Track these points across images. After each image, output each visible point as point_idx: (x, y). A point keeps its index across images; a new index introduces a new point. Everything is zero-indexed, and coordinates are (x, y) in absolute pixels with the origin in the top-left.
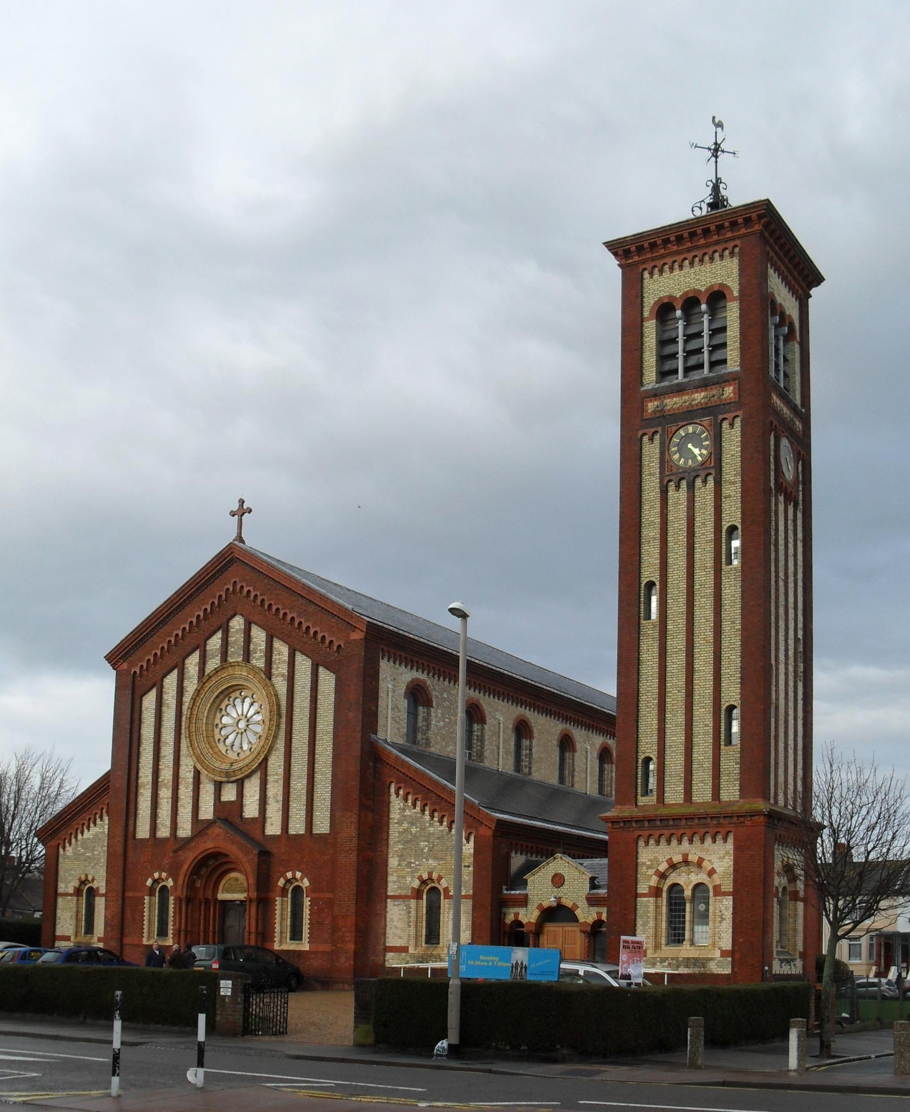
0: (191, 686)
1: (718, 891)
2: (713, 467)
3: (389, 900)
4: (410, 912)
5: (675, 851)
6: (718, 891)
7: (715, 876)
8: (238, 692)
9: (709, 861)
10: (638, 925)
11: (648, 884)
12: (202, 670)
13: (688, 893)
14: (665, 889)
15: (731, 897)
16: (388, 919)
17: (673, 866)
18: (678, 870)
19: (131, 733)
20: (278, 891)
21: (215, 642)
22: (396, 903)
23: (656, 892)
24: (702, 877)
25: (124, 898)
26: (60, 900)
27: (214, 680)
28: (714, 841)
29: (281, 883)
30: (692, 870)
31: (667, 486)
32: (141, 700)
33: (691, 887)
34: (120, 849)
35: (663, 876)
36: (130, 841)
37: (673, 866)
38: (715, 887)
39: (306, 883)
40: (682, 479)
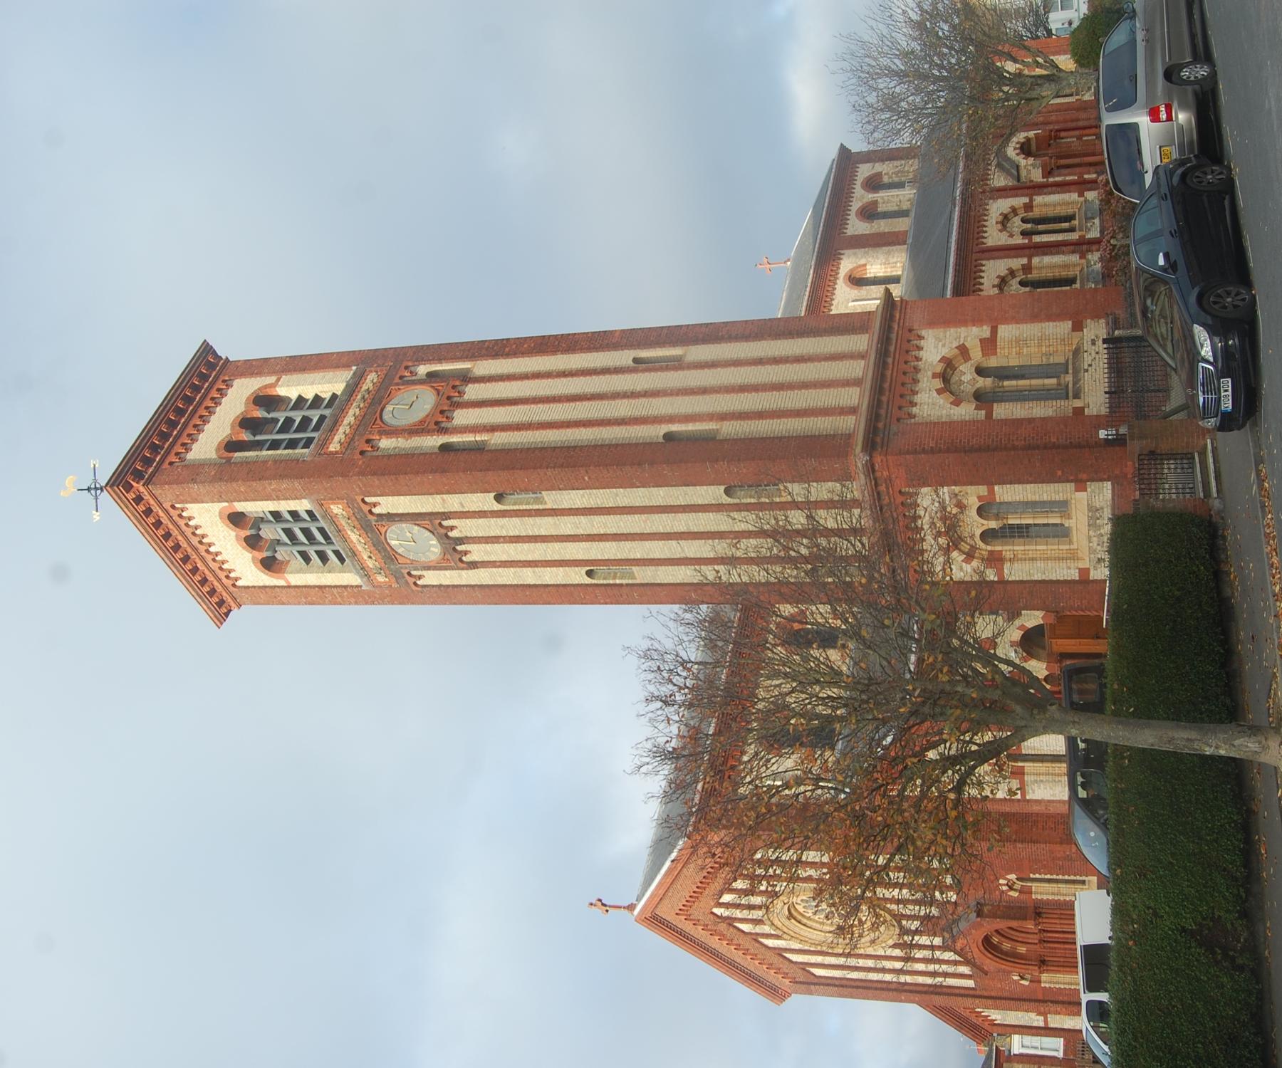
0: (796, 946)
2: (431, 521)
3: (1027, 798)
4: (1042, 781)
8: (797, 906)
10: (1044, 578)
12: (777, 937)
15: (996, 488)
16: (1052, 798)
19: (858, 987)
20: (1024, 897)
21: (746, 927)
22: (1030, 791)
25: (1046, 1002)
26: (1051, 1025)
27: (786, 930)
29: (1014, 894)
31: (467, 563)
32: (820, 977)
34: (990, 1002)
36: (978, 993)
39: (1013, 877)
40: (454, 549)
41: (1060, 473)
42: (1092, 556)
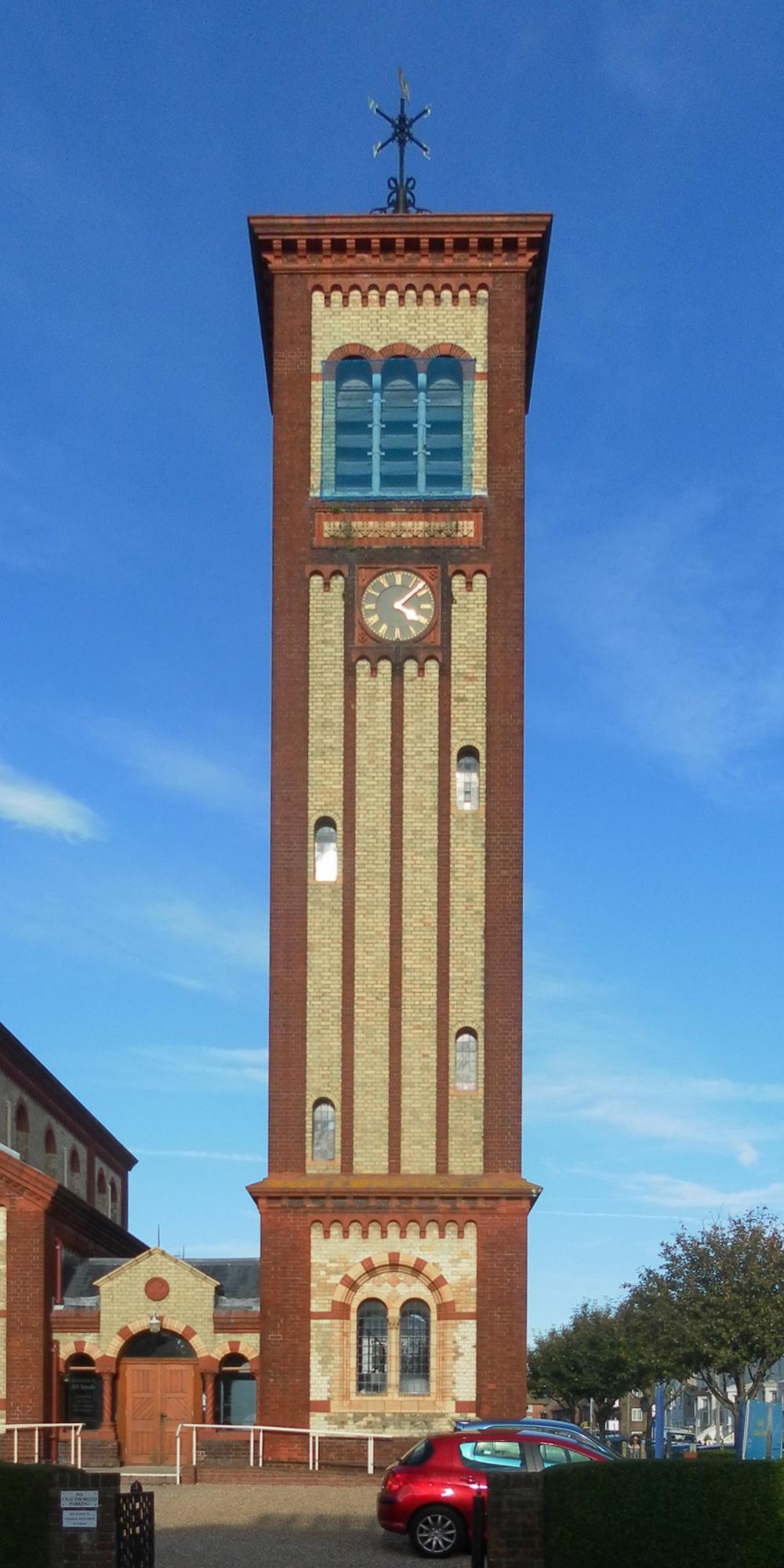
1: (447, 1312)
5: (377, 1247)
6: (447, 1312)
7: (444, 1289)
9: (434, 1264)
11: (331, 1298)
13: (394, 1313)
14: (355, 1305)
17: (371, 1270)
18: (376, 1278)
23: (340, 1311)
24: (418, 1289)
28: (442, 1235)
30: (401, 1279)
33: (399, 1304)
35: (352, 1285)
37: (371, 1270)
38: (439, 1307)
41: (491, 1386)
42: (351, 1415)
